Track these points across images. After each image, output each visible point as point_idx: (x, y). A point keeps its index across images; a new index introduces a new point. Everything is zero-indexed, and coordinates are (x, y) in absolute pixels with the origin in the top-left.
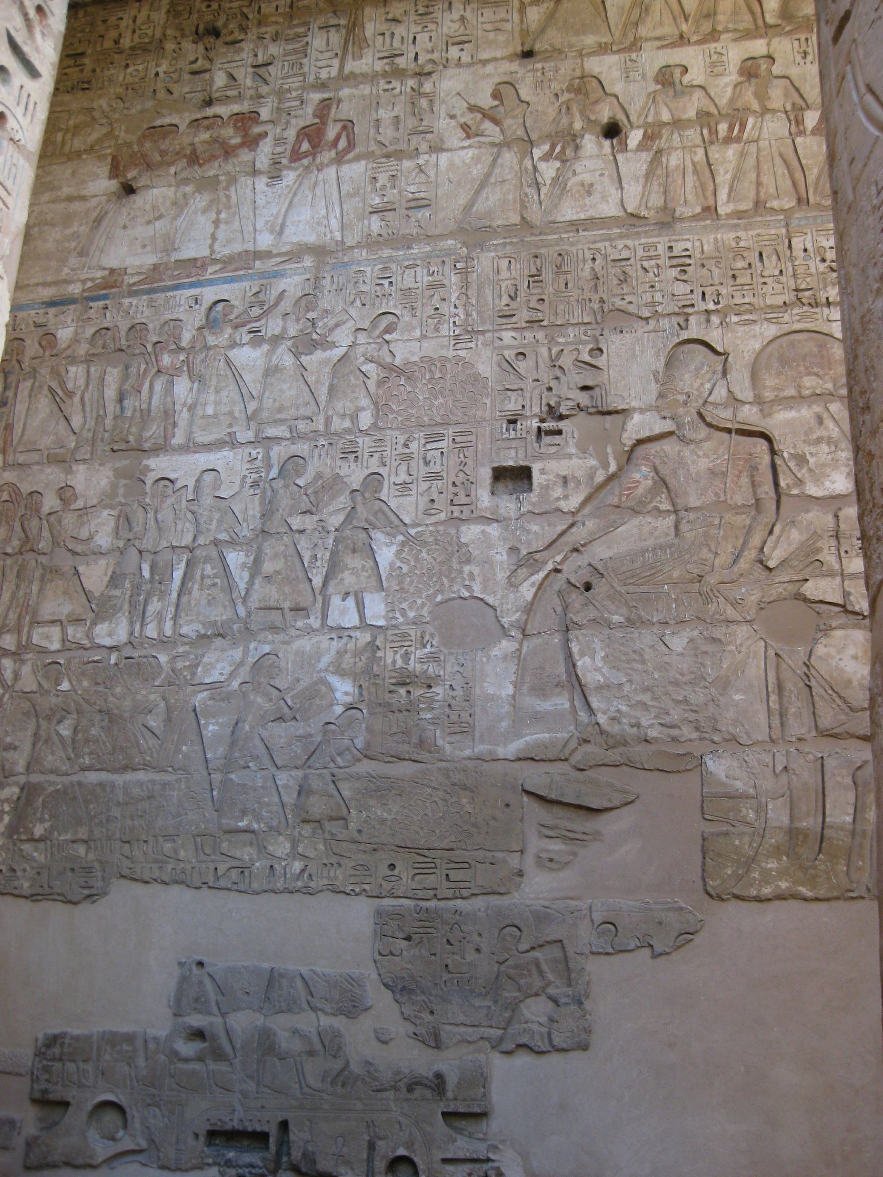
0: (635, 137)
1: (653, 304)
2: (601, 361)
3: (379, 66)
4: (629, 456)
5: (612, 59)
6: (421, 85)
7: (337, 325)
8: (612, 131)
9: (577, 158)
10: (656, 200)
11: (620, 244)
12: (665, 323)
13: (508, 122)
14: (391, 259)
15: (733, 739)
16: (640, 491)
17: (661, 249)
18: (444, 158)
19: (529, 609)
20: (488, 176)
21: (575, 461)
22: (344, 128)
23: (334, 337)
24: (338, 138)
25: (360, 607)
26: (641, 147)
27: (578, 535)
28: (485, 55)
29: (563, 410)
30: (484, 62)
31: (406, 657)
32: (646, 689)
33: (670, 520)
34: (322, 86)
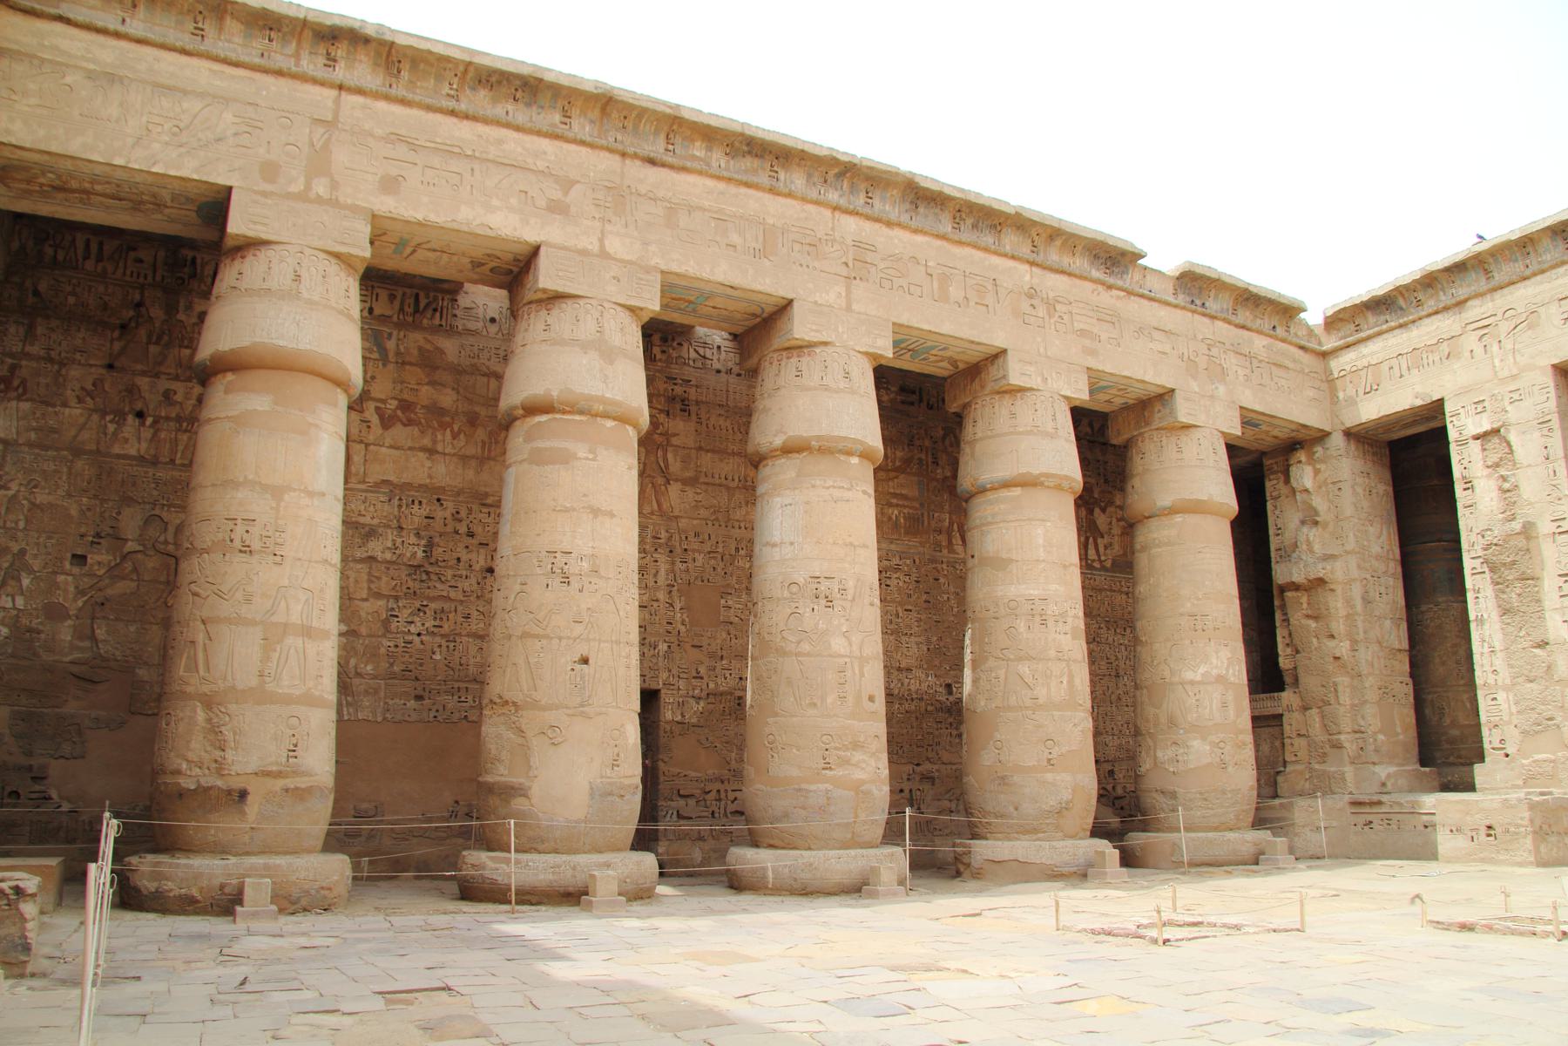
0: (149, 420)
1: (143, 497)
2: (120, 517)
3: (42, 353)
4: (124, 557)
5: (147, 380)
6: (60, 369)
7: (12, 480)
8: (140, 415)
9: (124, 424)
10: (152, 452)
11: (135, 468)
12: (147, 507)
13: (98, 399)
14: (38, 455)
15: (146, 663)
16: (127, 571)
17: (151, 474)
18: (67, 411)
19: (80, 610)
20: (86, 423)
21: (104, 557)
22: (22, 382)
23: (10, 485)
24: (18, 387)
25: (14, 600)
26: (151, 426)
27: (101, 584)
28: (92, 362)
29: (103, 535)
30: (91, 366)
31: (30, 622)
32: (118, 643)
33: (136, 583)
34: (12, 355)
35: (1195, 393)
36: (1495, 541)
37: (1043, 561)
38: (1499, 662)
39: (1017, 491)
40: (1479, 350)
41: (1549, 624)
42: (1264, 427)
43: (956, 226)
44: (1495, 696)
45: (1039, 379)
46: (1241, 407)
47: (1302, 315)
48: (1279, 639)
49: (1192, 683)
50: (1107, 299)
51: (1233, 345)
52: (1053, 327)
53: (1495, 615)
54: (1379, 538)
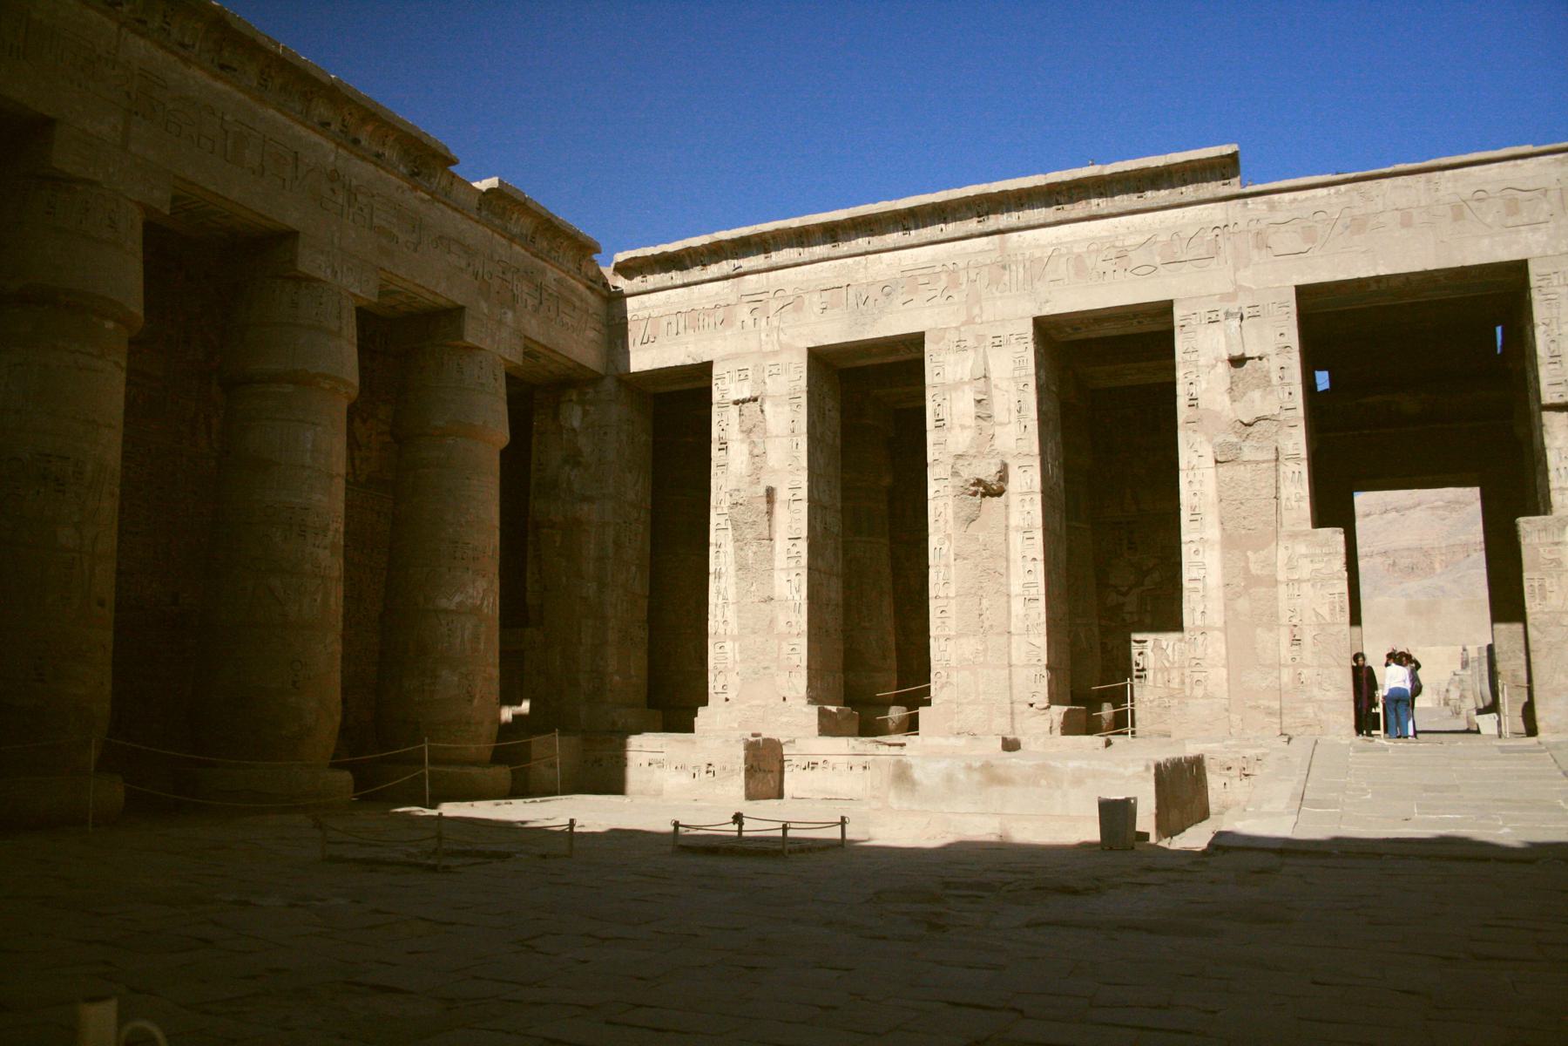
35: (484, 314)
36: (740, 501)
37: (309, 467)
38: (730, 613)
39: (289, 388)
40: (749, 321)
41: (777, 582)
42: (542, 361)
43: (262, 82)
44: (723, 644)
45: (329, 271)
46: (526, 337)
47: (595, 257)
48: (528, 575)
49: (447, 611)
50: (414, 199)
51: (526, 272)
52: (351, 217)
53: (732, 569)
54: (635, 485)
